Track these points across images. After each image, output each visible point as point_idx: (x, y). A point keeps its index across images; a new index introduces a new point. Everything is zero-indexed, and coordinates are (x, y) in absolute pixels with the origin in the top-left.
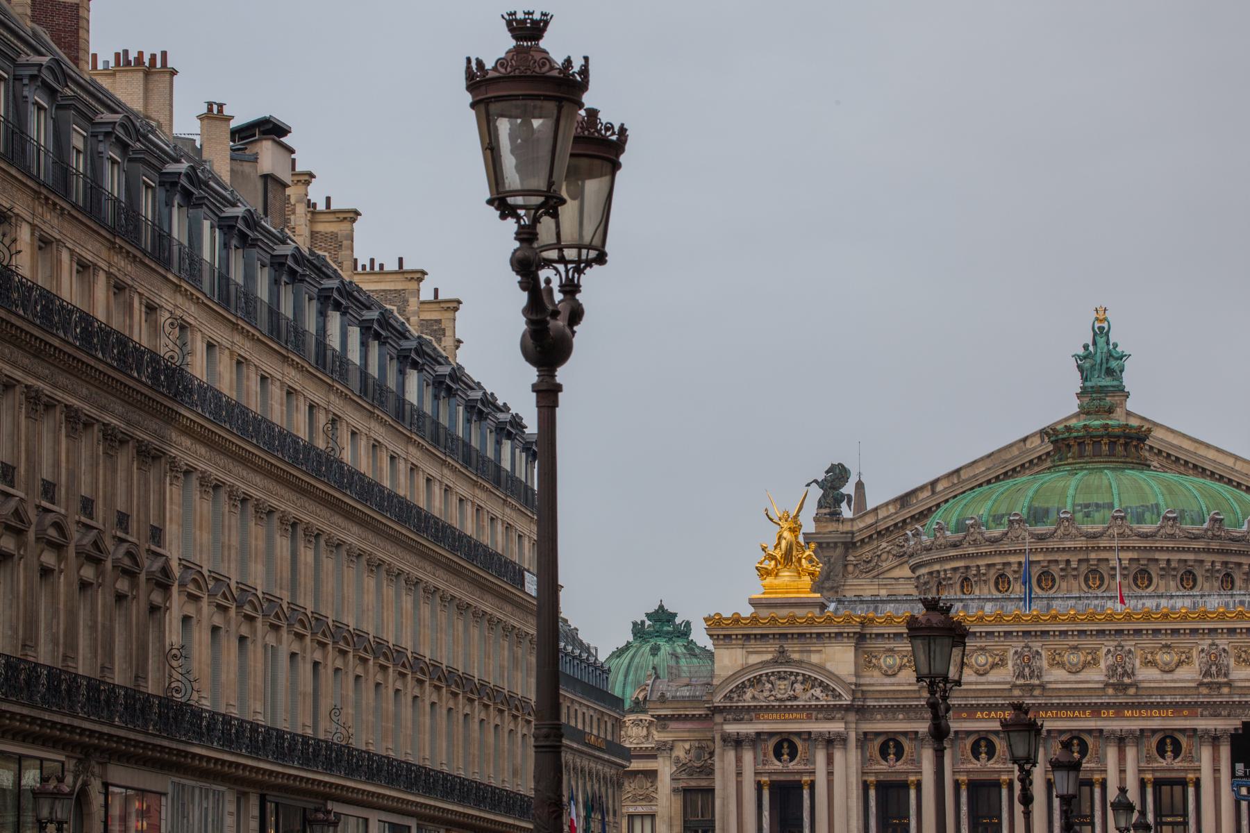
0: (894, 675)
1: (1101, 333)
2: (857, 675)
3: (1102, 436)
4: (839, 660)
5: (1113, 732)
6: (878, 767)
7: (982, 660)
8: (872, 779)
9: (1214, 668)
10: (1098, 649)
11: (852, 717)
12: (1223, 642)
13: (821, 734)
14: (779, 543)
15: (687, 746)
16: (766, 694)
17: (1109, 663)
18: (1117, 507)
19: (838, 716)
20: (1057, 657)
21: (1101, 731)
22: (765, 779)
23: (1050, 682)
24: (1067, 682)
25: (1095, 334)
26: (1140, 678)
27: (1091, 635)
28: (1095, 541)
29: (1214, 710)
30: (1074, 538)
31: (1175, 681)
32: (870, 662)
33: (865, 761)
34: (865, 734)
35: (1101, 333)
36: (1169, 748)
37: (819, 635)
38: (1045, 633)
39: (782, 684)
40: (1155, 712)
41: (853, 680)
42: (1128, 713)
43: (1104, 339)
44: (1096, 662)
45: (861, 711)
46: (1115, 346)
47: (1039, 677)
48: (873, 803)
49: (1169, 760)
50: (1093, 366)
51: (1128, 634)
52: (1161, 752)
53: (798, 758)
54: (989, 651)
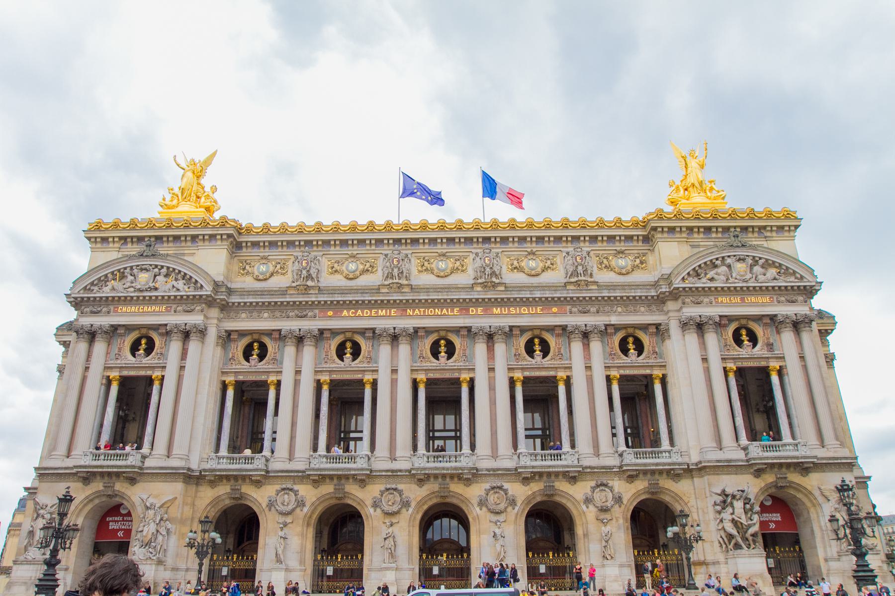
0: (265, 280)
2: (227, 277)
4: (212, 261)
7: (352, 267)
8: (230, 379)
9: (580, 268)
11: (214, 313)
12: (586, 247)
17: (476, 265)
19: (199, 308)
20: (426, 264)
21: (469, 329)
26: (507, 282)
29: (582, 304)
32: (244, 269)
34: (229, 333)
36: (537, 347)
37: (194, 238)
38: (415, 241)
40: (524, 310)
42: (496, 311)
45: (225, 308)
47: (407, 278)
52: (530, 351)
53: (153, 353)
54: (358, 259)
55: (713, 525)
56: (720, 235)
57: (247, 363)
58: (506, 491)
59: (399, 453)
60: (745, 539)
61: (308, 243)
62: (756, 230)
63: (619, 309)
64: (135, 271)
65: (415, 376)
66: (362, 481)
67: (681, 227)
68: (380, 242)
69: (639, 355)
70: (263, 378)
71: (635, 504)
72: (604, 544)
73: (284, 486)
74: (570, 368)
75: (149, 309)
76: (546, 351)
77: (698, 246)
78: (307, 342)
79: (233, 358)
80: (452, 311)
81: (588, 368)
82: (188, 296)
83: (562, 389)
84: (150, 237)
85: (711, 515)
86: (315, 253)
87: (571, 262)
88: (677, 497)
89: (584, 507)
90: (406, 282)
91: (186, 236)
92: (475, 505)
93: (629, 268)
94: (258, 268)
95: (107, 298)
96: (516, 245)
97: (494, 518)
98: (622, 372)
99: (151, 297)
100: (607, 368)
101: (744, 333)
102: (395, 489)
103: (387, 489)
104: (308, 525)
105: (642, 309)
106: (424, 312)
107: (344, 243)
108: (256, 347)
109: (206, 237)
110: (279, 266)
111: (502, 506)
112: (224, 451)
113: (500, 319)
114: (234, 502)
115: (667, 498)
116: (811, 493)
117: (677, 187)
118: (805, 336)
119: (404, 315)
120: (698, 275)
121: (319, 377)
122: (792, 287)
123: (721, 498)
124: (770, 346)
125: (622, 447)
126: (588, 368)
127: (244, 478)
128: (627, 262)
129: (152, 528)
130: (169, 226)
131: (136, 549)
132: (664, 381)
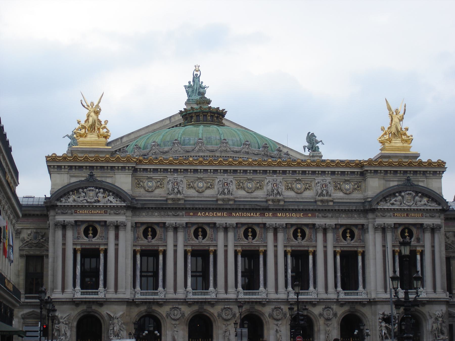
1: (196, 78)
2: (132, 190)
3: (208, 112)
5: (271, 225)
6: (142, 242)
8: (138, 248)
10: (263, 181)
11: (129, 213)
12: (328, 179)
13: (111, 222)
14: (88, 119)
15: (29, 232)
16: (81, 199)
18: (222, 138)
19: (123, 212)
20: (241, 184)
21: (265, 224)
22: (78, 247)
23: (237, 198)
24: (246, 198)
25: (194, 77)
26: (285, 196)
27: (260, 173)
28: (213, 153)
30: (203, 151)
31: (302, 198)
32: (139, 184)
33: (136, 239)
34: (136, 223)
35: (196, 78)
37: (112, 168)
38: (235, 171)
39: (92, 194)
40: (294, 215)
41: (130, 192)
43: (198, 79)
44: (260, 188)
46: (202, 83)
48: (138, 262)
49: (300, 241)
50: (193, 91)
51: (279, 173)
52: (295, 236)
53: (98, 236)
55: (378, 328)
56: (402, 175)
57: (146, 240)
58: (282, 310)
59: (229, 290)
60: (390, 335)
61: (176, 171)
62: (422, 172)
63: (344, 216)
64: (85, 190)
65: (236, 249)
66: (213, 304)
67: (381, 171)
68: (216, 171)
69: (352, 240)
70: (156, 248)
71: (343, 316)
72: (327, 335)
73: (174, 306)
74: (316, 246)
75: (95, 212)
76: (303, 236)
77: (390, 181)
78: (180, 230)
79: (138, 238)
80: (256, 214)
81: (325, 247)
82: (117, 206)
83: (311, 257)
84: (86, 166)
85: (378, 323)
86: (179, 177)
87: (319, 187)
88: (363, 315)
89: (319, 318)
90: (231, 197)
91: (107, 167)
92: (267, 316)
93: (351, 190)
94: (147, 184)
95: (71, 206)
96: (290, 175)
97: (276, 322)
98: (342, 249)
99: (96, 206)
100: (335, 247)
101: (406, 231)
102: (228, 308)
103: (225, 308)
104: (186, 325)
105: (356, 216)
106: (241, 214)
107: (196, 171)
108: (150, 230)
109: (120, 168)
110: (159, 183)
111: (280, 317)
112: (138, 288)
113: (281, 220)
114: (147, 313)
115: (358, 314)
116: (425, 314)
117: (385, 134)
118: (436, 236)
119: (230, 215)
120: (386, 201)
121: (186, 248)
122: (433, 209)
123: (382, 316)
124: (418, 240)
125: (339, 289)
126: (325, 247)
127: (153, 302)
128: (350, 186)
129: (118, 326)
130: (96, 161)
131: (112, 337)
132: (363, 254)
